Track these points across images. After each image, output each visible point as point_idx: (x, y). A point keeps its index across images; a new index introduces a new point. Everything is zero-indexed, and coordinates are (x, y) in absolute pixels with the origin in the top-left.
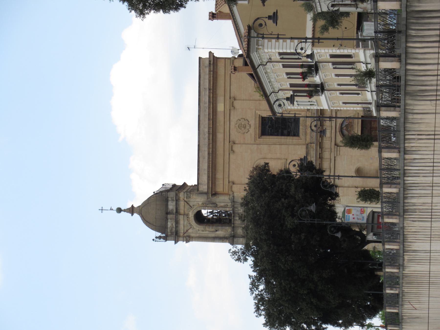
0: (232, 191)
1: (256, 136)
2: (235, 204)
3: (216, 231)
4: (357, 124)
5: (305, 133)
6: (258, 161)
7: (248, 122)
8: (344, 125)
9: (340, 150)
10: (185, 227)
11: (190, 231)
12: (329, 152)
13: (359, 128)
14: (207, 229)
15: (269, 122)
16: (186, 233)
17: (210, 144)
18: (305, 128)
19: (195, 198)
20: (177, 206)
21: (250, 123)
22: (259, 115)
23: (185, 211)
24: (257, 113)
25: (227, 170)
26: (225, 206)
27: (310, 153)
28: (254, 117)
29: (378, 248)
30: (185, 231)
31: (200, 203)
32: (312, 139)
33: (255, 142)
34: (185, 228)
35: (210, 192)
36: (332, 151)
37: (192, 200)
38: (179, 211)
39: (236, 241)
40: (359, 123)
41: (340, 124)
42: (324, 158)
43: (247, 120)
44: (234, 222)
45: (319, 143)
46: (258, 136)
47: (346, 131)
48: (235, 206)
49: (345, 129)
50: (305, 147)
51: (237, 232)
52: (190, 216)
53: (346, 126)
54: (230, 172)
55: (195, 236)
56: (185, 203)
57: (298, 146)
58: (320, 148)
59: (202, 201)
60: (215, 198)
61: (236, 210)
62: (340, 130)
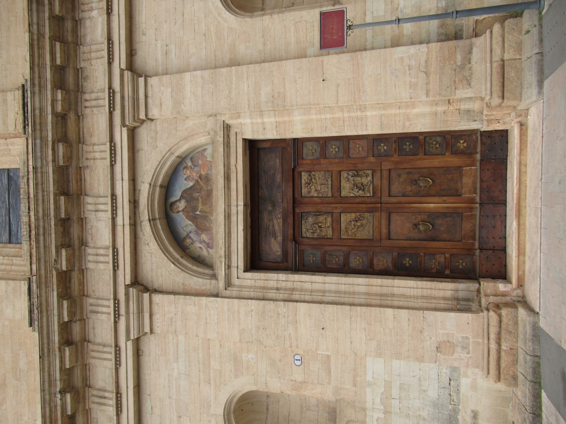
8: (177, 194)
9: (155, 308)
13: (234, 202)
40: (233, 176)
41: (152, 186)
45: (54, 273)
47: (188, 217)
49: (183, 210)
53: (187, 194)
58: (61, 297)
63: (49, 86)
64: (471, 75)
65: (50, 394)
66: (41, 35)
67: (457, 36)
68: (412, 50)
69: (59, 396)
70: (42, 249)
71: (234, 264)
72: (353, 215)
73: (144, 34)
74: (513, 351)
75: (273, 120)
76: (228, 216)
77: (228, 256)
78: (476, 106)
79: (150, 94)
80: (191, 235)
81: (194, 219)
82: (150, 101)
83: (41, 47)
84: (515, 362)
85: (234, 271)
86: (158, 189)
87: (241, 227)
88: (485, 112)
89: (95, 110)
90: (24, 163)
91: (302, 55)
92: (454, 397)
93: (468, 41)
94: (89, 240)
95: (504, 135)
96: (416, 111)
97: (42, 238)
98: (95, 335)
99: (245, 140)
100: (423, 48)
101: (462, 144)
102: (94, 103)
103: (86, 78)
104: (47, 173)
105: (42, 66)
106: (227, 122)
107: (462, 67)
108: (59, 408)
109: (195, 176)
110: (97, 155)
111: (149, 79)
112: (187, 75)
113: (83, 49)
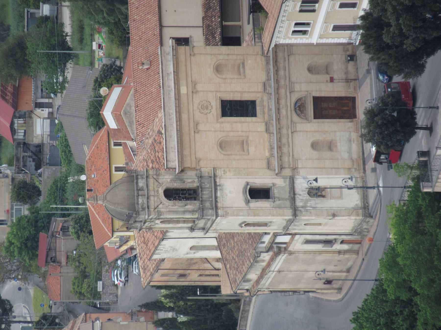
3: (186, 205)
11: (161, 206)
21: (211, 104)
31: (169, 180)
37: (160, 177)
43: (209, 102)
53: (299, 106)
58: (279, 123)
67: (348, 82)
81: (300, 111)
91: (323, 82)
101: (349, 99)
109: (300, 103)
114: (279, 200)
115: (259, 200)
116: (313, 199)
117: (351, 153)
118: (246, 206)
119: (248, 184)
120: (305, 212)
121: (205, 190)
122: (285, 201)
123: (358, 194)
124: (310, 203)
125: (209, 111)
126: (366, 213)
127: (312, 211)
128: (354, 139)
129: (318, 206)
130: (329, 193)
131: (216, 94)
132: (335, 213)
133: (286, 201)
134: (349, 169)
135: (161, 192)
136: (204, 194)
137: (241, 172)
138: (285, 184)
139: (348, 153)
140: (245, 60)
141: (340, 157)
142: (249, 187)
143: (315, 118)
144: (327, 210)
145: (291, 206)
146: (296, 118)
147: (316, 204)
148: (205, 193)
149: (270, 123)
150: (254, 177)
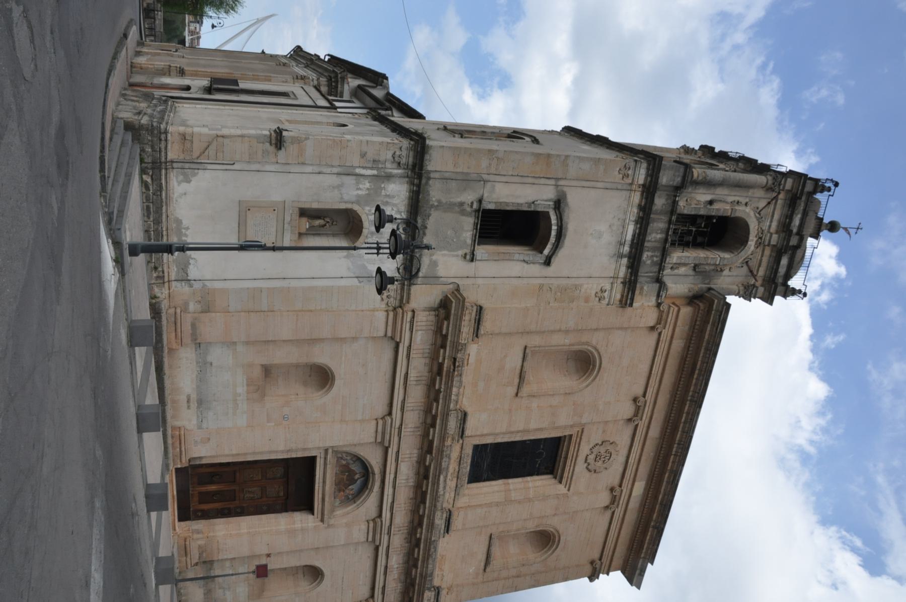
0: (661, 313)
1: (578, 440)
2: (655, 272)
3: (711, 202)
4: (327, 499)
5: (462, 462)
6: (585, 384)
7: (589, 467)
8: (359, 482)
9: (373, 435)
10: (771, 214)
11: (762, 204)
12: (405, 428)
14: (728, 207)
15: (539, 464)
16: (772, 200)
17: (685, 422)
18: (461, 471)
19: (734, 284)
20: (775, 267)
21: (586, 465)
22: (560, 482)
23: (760, 254)
24: (565, 487)
25: (659, 360)
26: (677, 266)
27: (457, 422)
28: (574, 478)
29: (268, 144)
30: (772, 206)
31: (726, 272)
32: (448, 452)
33: (583, 428)
34: (772, 209)
35: (713, 312)
36: (397, 430)
37: (740, 279)
38: (774, 254)
39: (679, 176)
41: (371, 490)
42: (420, 410)
43: (590, 471)
44: (667, 225)
45: (434, 455)
46: (574, 439)
47: (354, 471)
48: (658, 267)
49: (357, 474)
50: (468, 432)
51: (667, 200)
52: (755, 239)
53: (353, 481)
54: (651, 353)
55: (756, 190)
56: (755, 273)
57: (485, 432)
59: (722, 278)
60: (696, 288)
61: (657, 257)
62: (371, 475)
63: (422, 541)
64: (199, 549)
65: (447, 392)
66: (423, 562)
68: (225, 557)
69: (442, 390)
70: (438, 469)
71: (322, 460)
72: (255, 479)
73: (369, 557)
74: (174, 448)
75: (296, 526)
76: (324, 482)
77: (325, 464)
78: (196, 536)
79: (366, 534)
80: (352, 462)
82: (366, 531)
83: (424, 557)
84: (173, 444)
85: (323, 456)
86: (369, 487)
87: (317, 477)
88: (191, 534)
89: (401, 525)
90: (458, 494)
92: (199, 413)
93: (201, 561)
94: (415, 464)
95: (180, 520)
96: (223, 533)
97: (437, 474)
98: (419, 414)
99: (313, 514)
100: (220, 558)
101: (200, 514)
102: (402, 529)
103: (406, 538)
104: (429, 503)
105: (425, 549)
106: (322, 523)
107: (203, 552)
108: (443, 383)
109: (347, 491)
110: (403, 505)
111: (365, 540)
112: (342, 543)
113: (406, 552)
114: (462, 204)
115: (525, 208)
116: (349, 206)
117: (198, 363)
118: (565, 189)
119: (548, 262)
120: (382, 158)
121: (656, 244)
122: (444, 201)
123: (179, 222)
124: (360, 192)
125: (595, 451)
126: (152, 147)
127: (356, 160)
128: (189, 407)
129: (334, 180)
130: (286, 226)
131: (569, 490)
132: (272, 149)
133: (439, 201)
134: (207, 310)
135: (752, 240)
136: (660, 233)
137: (559, 294)
138: (434, 258)
139: (211, 364)
140: (481, 571)
141: (240, 348)
142: (546, 251)
143: (312, 460)
144: (303, 164)
145: (427, 183)
146: (374, 459)
147: (339, 187)
148: (659, 236)
149: (453, 439)
150: (525, 281)
